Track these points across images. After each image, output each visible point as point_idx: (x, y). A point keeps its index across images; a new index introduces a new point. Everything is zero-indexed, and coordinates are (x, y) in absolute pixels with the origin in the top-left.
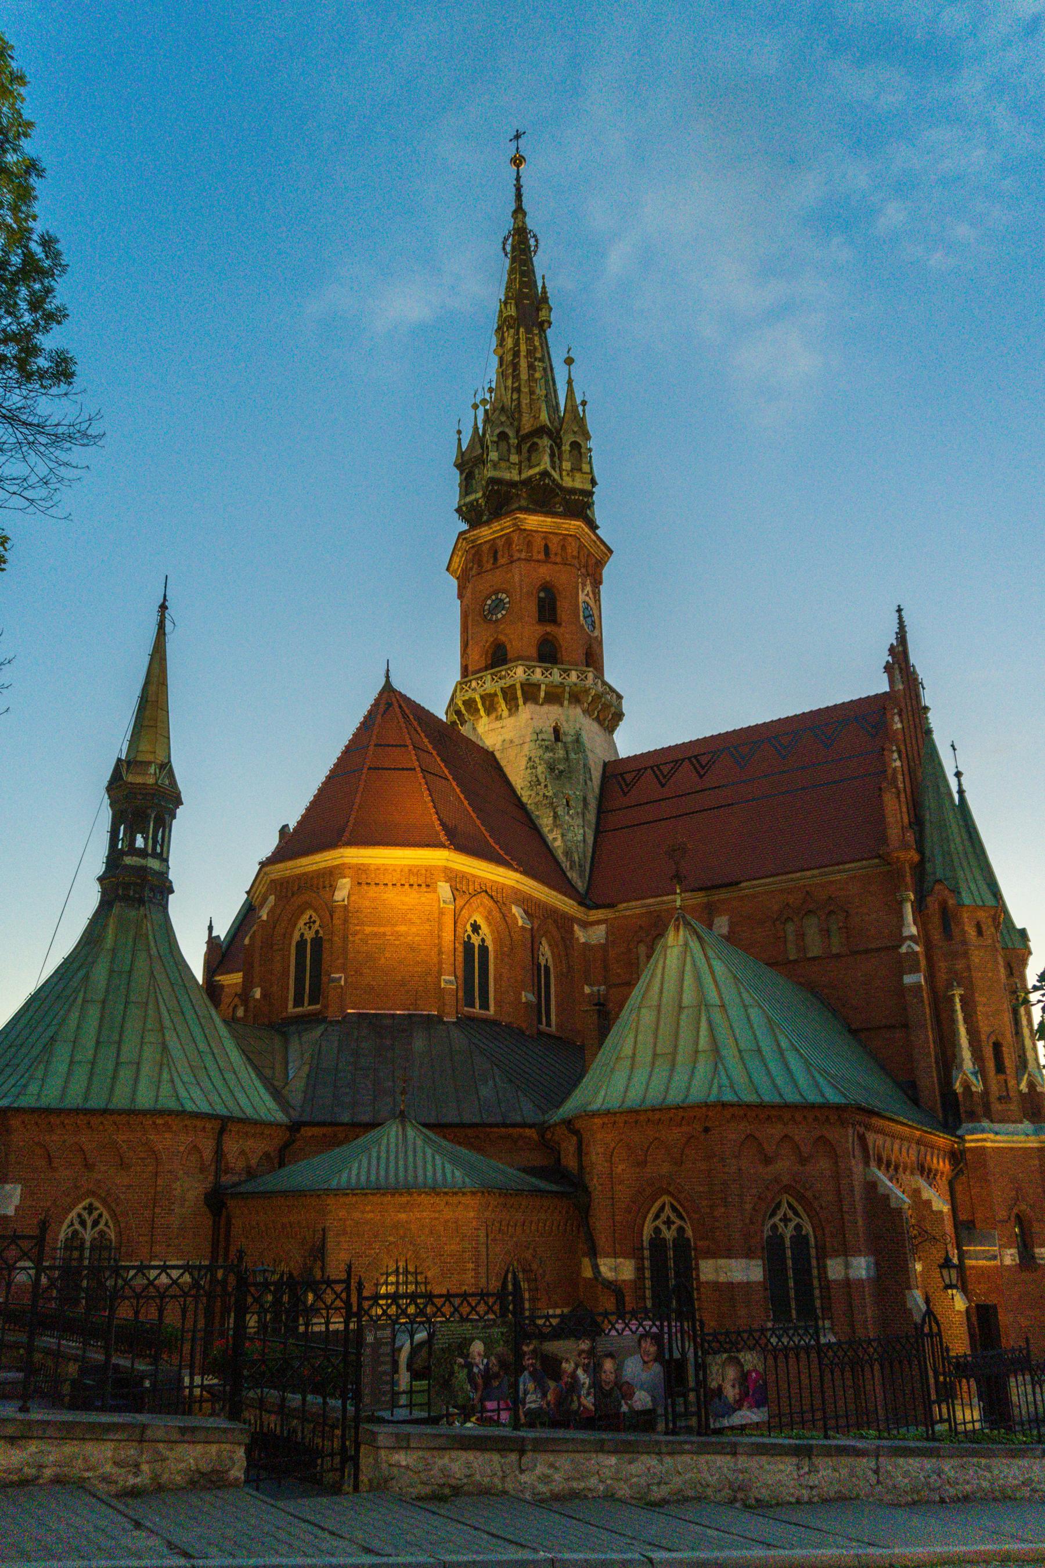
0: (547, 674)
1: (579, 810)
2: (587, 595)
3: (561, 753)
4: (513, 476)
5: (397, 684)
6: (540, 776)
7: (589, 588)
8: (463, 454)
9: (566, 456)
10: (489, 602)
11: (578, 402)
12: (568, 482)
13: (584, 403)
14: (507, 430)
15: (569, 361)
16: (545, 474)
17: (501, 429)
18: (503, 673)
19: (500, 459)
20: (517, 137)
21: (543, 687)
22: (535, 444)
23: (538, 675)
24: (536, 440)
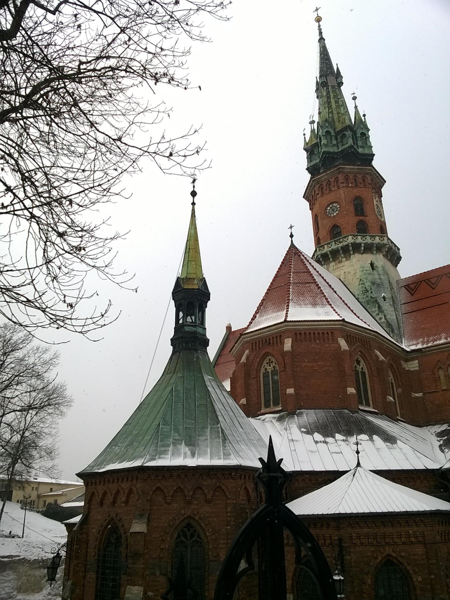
0: (364, 239)
3: (376, 276)
4: (335, 150)
6: (367, 288)
7: (377, 199)
8: (307, 144)
9: (359, 139)
10: (329, 208)
13: (364, 115)
14: (330, 130)
16: (351, 147)
18: (341, 240)
20: (317, 10)
21: (363, 245)
23: (359, 240)
24: (344, 132)
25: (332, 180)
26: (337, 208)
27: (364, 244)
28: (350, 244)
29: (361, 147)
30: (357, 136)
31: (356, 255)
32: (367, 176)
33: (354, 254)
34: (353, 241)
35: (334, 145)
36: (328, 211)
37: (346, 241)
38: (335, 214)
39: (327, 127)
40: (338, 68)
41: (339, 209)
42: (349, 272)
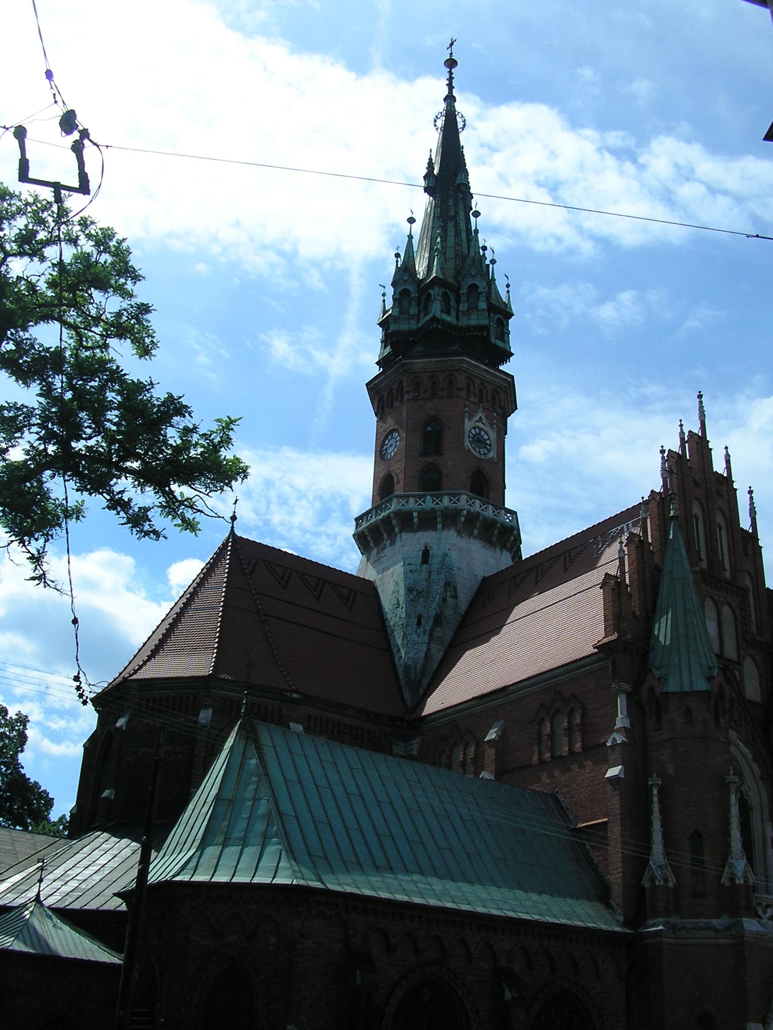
0: (420, 502)
1: (428, 628)
2: (480, 420)
4: (413, 325)
12: (464, 322)
14: (408, 287)
17: (403, 287)
18: (384, 506)
19: (400, 313)
21: (415, 514)
22: (429, 295)
23: (412, 504)
27: (418, 512)
30: (461, 292)
31: (405, 536)
33: (400, 532)
34: (399, 507)
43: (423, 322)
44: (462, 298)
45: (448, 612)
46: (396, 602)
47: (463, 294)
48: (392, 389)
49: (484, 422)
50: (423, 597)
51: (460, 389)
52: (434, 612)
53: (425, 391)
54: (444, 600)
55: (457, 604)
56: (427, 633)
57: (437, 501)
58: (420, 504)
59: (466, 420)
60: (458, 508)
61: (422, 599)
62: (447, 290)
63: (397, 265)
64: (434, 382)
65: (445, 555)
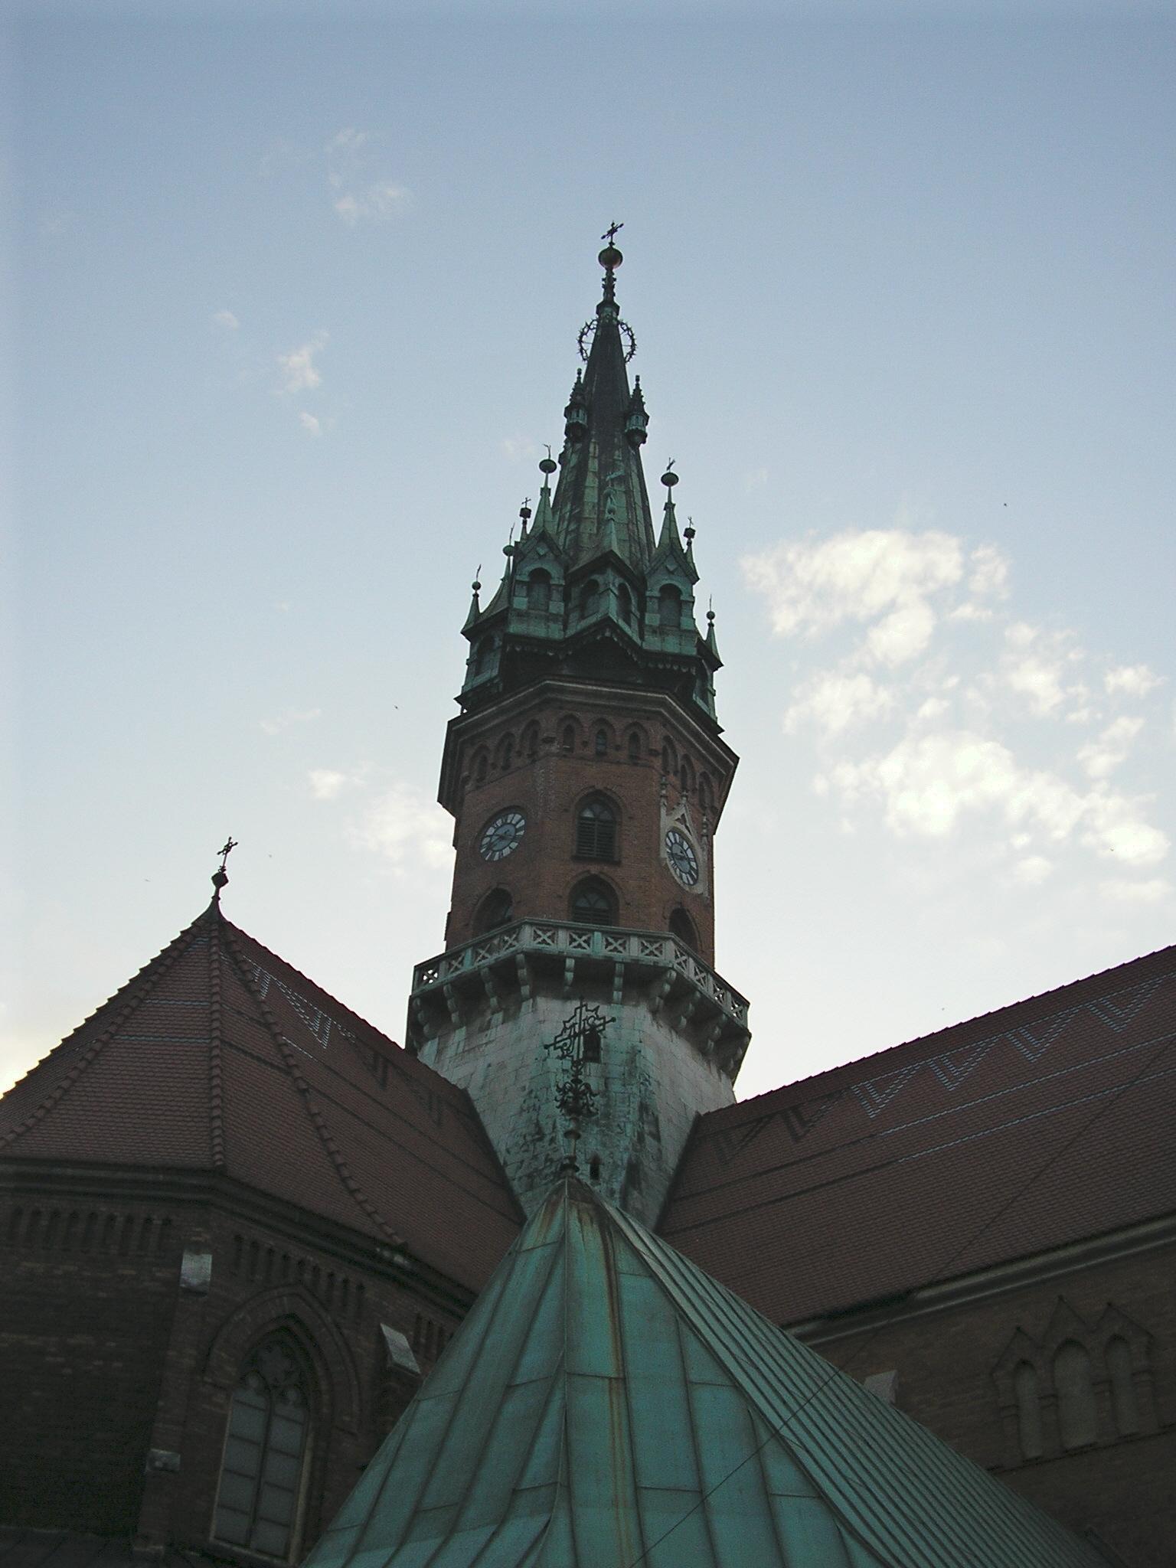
1: (616, 1186)
2: (682, 820)
4: (556, 632)
5: (230, 912)
6: (543, 1123)
9: (653, 605)
11: (681, 533)
12: (652, 643)
13: (690, 533)
14: (546, 567)
15: (670, 480)
17: (537, 565)
18: (496, 942)
21: (570, 963)
23: (562, 943)
25: (517, 731)
26: (517, 830)
28: (520, 957)
29: (654, 632)
30: (648, 593)
32: (647, 725)
33: (533, 995)
35: (550, 618)
36: (486, 840)
37: (511, 946)
38: (506, 852)
39: (541, 557)
40: (638, 390)
41: (522, 833)
42: (502, 1066)
43: (579, 627)
44: (649, 604)
45: (649, 1165)
46: (532, 1129)
47: (651, 597)
48: (509, 735)
49: (688, 825)
50: (597, 1123)
51: (653, 753)
52: (626, 1156)
53: (585, 744)
54: (641, 1138)
55: (660, 1151)
56: (617, 1196)
57: (615, 945)
58: (580, 946)
59: (663, 811)
60: (661, 965)
61: (596, 1129)
62: (627, 584)
63: (524, 528)
64: (602, 732)
65: (634, 1053)
